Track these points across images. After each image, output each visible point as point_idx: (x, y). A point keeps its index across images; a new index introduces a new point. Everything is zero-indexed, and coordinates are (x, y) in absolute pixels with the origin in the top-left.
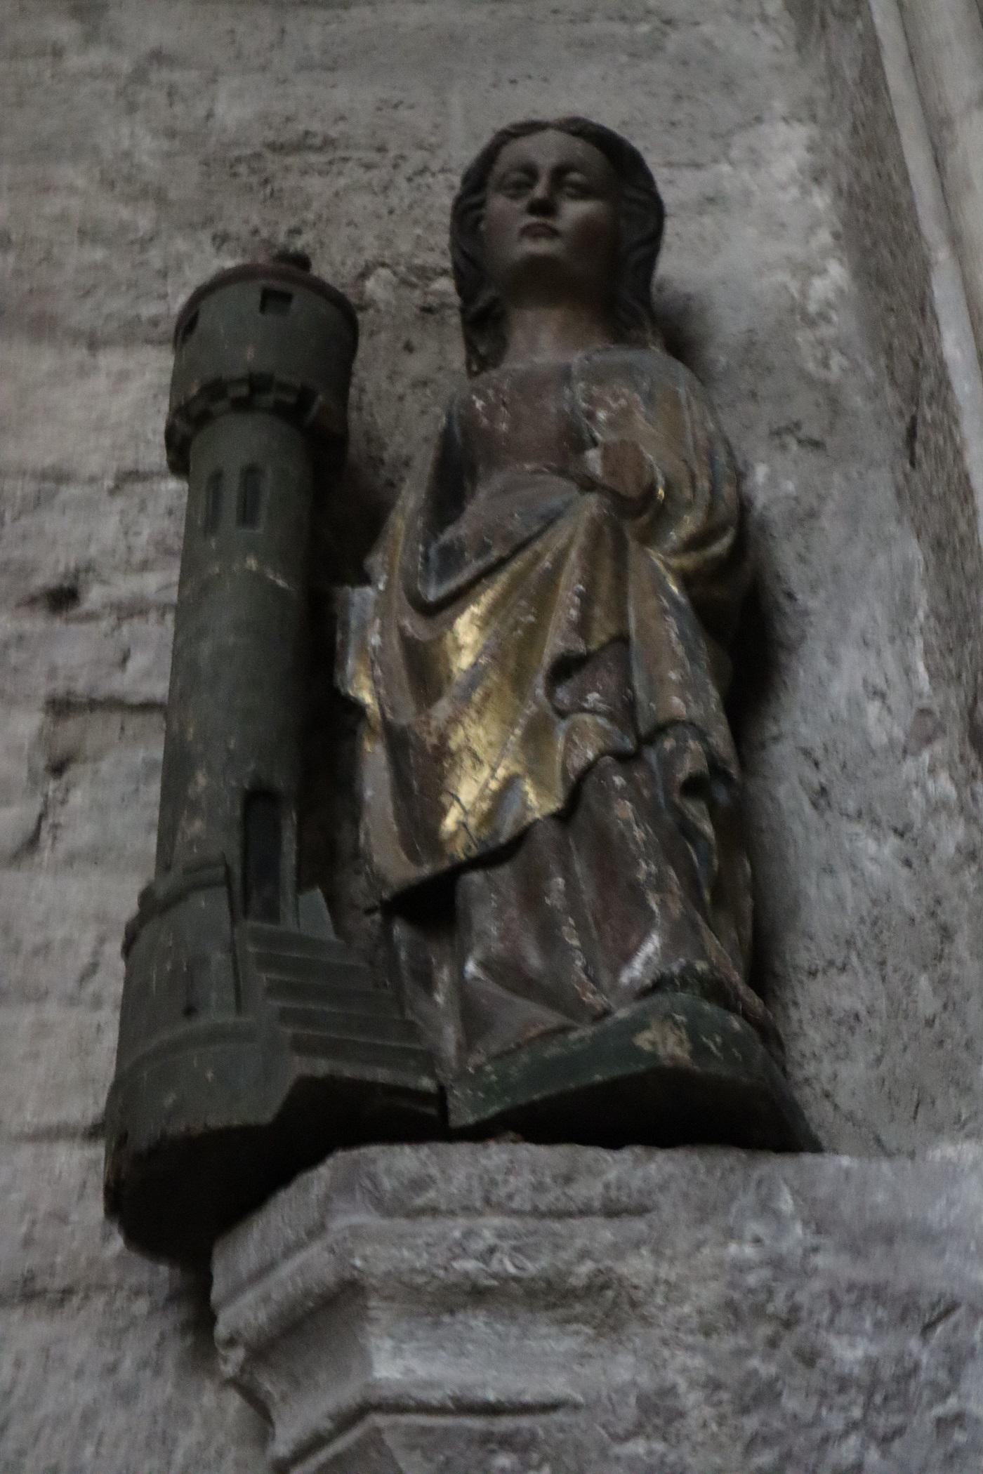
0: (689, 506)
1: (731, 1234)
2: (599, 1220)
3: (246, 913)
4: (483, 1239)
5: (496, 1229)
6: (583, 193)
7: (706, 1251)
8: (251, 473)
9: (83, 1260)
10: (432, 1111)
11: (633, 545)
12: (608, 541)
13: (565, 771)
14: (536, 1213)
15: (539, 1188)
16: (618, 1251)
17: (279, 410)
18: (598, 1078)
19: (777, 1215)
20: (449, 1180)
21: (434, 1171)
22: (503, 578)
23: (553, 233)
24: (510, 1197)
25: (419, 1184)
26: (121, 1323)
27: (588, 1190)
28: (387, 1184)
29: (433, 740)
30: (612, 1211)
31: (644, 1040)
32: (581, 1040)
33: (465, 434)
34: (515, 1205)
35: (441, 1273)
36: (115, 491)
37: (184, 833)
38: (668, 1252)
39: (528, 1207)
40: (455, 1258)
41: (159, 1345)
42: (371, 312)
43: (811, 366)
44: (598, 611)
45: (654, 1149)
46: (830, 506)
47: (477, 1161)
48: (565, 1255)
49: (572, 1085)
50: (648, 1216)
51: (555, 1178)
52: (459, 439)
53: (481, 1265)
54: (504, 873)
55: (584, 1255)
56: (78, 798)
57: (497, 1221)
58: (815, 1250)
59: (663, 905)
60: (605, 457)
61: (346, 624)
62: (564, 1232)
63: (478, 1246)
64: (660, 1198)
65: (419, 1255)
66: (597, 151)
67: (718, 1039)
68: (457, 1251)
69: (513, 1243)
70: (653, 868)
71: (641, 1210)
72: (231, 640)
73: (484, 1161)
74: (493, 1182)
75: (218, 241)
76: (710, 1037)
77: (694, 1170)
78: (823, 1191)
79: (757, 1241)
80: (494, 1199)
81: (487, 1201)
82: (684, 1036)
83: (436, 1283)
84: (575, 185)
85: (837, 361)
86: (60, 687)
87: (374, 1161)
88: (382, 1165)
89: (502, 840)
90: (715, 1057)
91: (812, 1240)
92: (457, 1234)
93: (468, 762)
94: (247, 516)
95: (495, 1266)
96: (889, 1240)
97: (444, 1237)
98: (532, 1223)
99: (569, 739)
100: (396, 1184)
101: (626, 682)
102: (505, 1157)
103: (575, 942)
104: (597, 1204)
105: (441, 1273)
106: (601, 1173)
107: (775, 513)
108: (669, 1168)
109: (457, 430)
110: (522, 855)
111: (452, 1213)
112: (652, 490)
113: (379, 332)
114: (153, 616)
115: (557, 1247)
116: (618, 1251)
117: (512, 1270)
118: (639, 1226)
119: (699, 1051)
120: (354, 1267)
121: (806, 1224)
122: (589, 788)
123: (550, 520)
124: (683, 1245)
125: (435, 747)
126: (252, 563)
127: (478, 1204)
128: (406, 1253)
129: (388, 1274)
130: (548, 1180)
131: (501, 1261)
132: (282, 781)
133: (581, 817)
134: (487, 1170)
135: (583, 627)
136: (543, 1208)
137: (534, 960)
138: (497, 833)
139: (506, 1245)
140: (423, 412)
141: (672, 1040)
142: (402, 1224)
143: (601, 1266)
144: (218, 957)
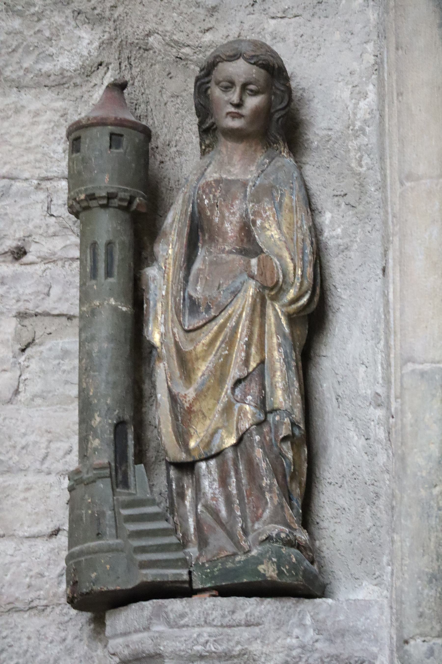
0: (292, 285)
1: (288, 634)
2: (243, 628)
3: (117, 487)
4: (204, 637)
5: (209, 633)
6: (255, 93)
7: (279, 641)
8: (109, 244)
9: (51, 594)
10: (187, 585)
11: (268, 302)
12: (258, 307)
13: (237, 429)
14: (222, 626)
15: (223, 616)
16: (249, 641)
17: (120, 207)
18: (245, 580)
20: (192, 614)
21: (187, 610)
22: (215, 327)
23: (240, 116)
24: (213, 620)
25: (182, 616)
26: (66, 618)
27: (240, 616)
28: (172, 616)
29: (187, 405)
30: (248, 625)
31: (261, 568)
32: (239, 562)
33: (199, 212)
34: (215, 623)
35: (190, 651)
36: (38, 187)
37: (92, 444)
38: (266, 642)
39: (219, 624)
40: (195, 645)
41: (81, 629)
42: (151, 52)
43: (354, 164)
44: (253, 350)
45: (263, 599)
46: (355, 246)
47: (202, 606)
48: (232, 644)
49: (236, 582)
50: (260, 627)
51: (229, 612)
52: (197, 215)
53: (203, 648)
54: (212, 462)
55: (238, 643)
56: (34, 365)
57: (209, 629)
58: (317, 641)
59: (271, 498)
60: (258, 265)
61: (148, 299)
62: (232, 634)
63: (202, 640)
65: (182, 645)
66: (262, 71)
67: (287, 567)
68: (195, 642)
69: (214, 638)
70: (268, 482)
71: (258, 624)
72: (105, 345)
73: (205, 606)
74: (208, 614)
75: (76, 14)
76: (284, 567)
77: (277, 608)
78: (321, 616)
79: (297, 637)
80: (208, 621)
81: (205, 622)
82: (275, 568)
83: (188, 654)
84: (251, 91)
85: (366, 160)
86: (22, 307)
87: (166, 607)
88: (170, 608)
89: (213, 453)
90: (285, 575)
91: (317, 637)
92: (195, 635)
93: (201, 416)
94: (109, 274)
95: (208, 648)
96: (343, 635)
97: (191, 637)
98: (220, 629)
99: (239, 415)
100: (174, 615)
101: (263, 387)
102: (212, 603)
103: (239, 513)
104: (243, 622)
105: (190, 651)
106: (245, 609)
107: (331, 243)
108: (268, 607)
109: (196, 209)
110: (220, 457)
111: (193, 626)
112: (278, 282)
113: (155, 65)
115: (229, 640)
116: (249, 641)
117: (213, 649)
118: (257, 630)
119: (280, 573)
120: (161, 650)
121: (314, 630)
122: (245, 437)
123: (235, 294)
124: (272, 639)
125: (188, 408)
126: (112, 301)
128: (178, 644)
129: (172, 652)
130: (226, 613)
131: (210, 646)
132: (127, 417)
133: (242, 445)
134: (205, 609)
135: (246, 362)
136: (224, 624)
137: (223, 512)
139: (212, 639)
140: (177, 113)
141: (271, 569)
143: (244, 648)
144: (109, 513)
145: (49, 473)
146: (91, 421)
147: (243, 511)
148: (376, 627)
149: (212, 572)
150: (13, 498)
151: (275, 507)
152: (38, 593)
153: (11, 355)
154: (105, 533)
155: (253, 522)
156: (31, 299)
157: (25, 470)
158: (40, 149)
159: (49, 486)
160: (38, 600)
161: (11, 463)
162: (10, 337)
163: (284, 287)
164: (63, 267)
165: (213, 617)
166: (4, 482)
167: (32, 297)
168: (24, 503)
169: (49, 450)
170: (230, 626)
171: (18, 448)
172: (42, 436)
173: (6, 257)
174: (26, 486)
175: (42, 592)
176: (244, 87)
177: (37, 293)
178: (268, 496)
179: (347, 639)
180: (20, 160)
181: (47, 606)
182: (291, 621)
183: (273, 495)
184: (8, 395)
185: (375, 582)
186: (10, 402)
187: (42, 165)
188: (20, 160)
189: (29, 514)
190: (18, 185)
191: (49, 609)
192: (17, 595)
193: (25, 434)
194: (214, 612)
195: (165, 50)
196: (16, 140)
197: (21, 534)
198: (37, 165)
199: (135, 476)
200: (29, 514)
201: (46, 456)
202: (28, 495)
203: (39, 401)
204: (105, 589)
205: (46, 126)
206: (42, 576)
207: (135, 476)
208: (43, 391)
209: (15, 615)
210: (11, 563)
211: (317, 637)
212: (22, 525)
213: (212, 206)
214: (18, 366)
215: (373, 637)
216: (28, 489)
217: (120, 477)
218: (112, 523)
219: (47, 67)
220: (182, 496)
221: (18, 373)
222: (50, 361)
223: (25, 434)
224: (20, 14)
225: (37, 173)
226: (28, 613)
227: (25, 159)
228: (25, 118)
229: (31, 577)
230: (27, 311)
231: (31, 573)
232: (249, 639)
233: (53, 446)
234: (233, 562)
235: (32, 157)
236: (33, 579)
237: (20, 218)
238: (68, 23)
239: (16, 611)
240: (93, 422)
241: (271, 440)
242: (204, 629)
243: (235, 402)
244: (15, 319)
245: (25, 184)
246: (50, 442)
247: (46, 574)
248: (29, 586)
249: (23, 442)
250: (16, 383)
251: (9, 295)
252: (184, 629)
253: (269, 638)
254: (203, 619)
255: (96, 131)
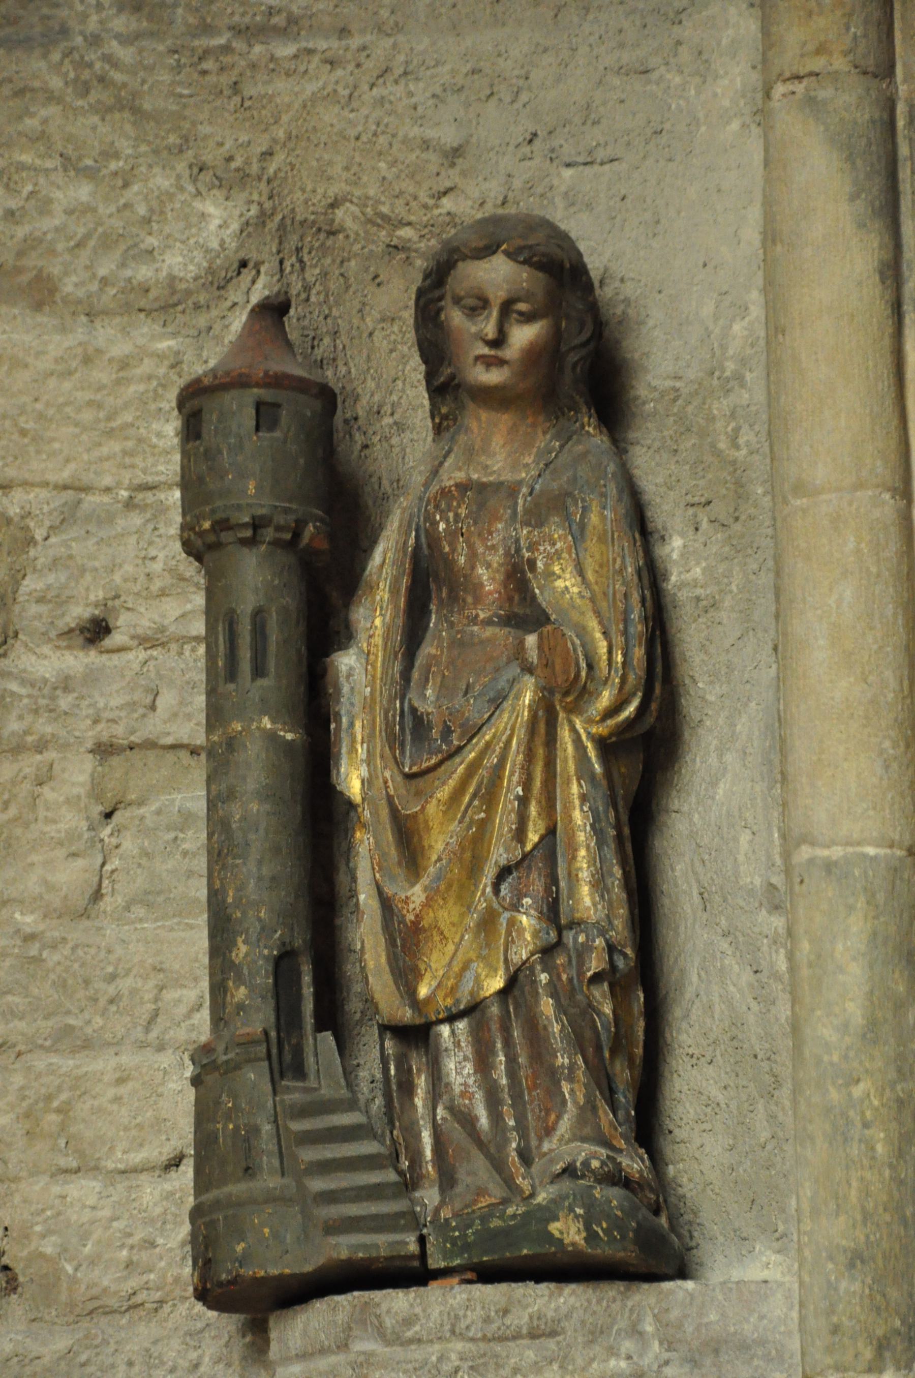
1: (612, 1352)
3: (282, 1076)
6: (528, 318)
8: (258, 615)
9: (170, 1279)
10: (416, 1263)
11: (562, 715)
13: (506, 960)
14: (484, 1338)
15: (487, 1320)
18: (525, 1251)
19: (641, 1334)
20: (428, 1317)
21: (418, 1310)
23: (501, 362)
24: (468, 1328)
25: (408, 1322)
26: (199, 1325)
27: (520, 1319)
28: (388, 1322)
29: (410, 917)
30: (534, 1335)
31: (555, 1228)
32: (514, 1216)
34: (471, 1334)
36: (129, 504)
37: (233, 996)
38: (570, 1367)
39: (479, 1335)
41: (227, 1345)
42: (341, 236)
44: (533, 810)
45: (563, 1285)
47: (447, 1302)
51: (497, 1312)
52: (426, 551)
54: (462, 1025)
56: (129, 844)
57: (459, 1346)
58: (667, 1363)
59: (572, 1091)
60: (540, 647)
61: (338, 715)
62: (504, 1354)
64: (565, 1324)
66: (540, 275)
67: (604, 1225)
69: (470, 1364)
70: (566, 1061)
71: (553, 1334)
72: (254, 807)
73: (451, 1301)
74: (457, 1317)
75: (195, 170)
76: (600, 1225)
77: (589, 1301)
78: (675, 1314)
79: (629, 1358)
80: (457, 1331)
81: (453, 1332)
82: (581, 1227)
84: (521, 313)
86: (103, 732)
87: (378, 1305)
88: (384, 1307)
90: (601, 1239)
91: (666, 1355)
92: (434, 1358)
93: (437, 938)
94: (259, 671)
96: (716, 1351)
97: (426, 1362)
99: (509, 933)
101: (553, 879)
102: (464, 1296)
103: (512, 1123)
104: (524, 1331)
106: (527, 1306)
107: (683, 595)
108: (572, 1300)
109: (423, 539)
110: (477, 1014)
111: (431, 1341)
113: (349, 260)
114: (174, 647)
115: (498, 1366)
119: (591, 1237)
121: (661, 1343)
122: (521, 976)
123: (497, 702)
124: (580, 1362)
125: (412, 922)
126: (267, 723)
127: (448, 1335)
130: (493, 1314)
132: (298, 943)
133: (516, 992)
136: (489, 1335)
137: (484, 1121)
138: (458, 1001)
139: (466, 1365)
140: (391, 351)
141: (573, 1230)
142: (398, 1352)
144: (267, 1128)
145: (161, 1048)
146: (230, 952)
147: (521, 1120)
148: (780, 1333)
149: (464, 1236)
150: (95, 1098)
151: (581, 1109)
152: (145, 1278)
153: (84, 825)
154: (260, 1168)
155: (540, 1140)
156: (120, 718)
157: (117, 1044)
158: (132, 432)
159: (161, 1073)
160: (145, 1292)
161: (89, 1030)
162: (81, 791)
163: (591, 687)
164: (180, 654)
165: (468, 1321)
166: (78, 1067)
167: (123, 714)
168: (115, 1107)
169: (160, 1004)
170: (502, 1339)
171: (102, 1002)
172: (145, 978)
173: (71, 639)
174: (117, 1075)
175: (152, 1276)
176: (506, 308)
177: (132, 706)
178: (566, 1087)
179: (724, 1358)
180: (96, 454)
181: (161, 1302)
182: (616, 1328)
183: (576, 1086)
184: (81, 902)
185: (776, 1245)
186: (85, 914)
187: (138, 460)
188: (96, 454)
189: (126, 1129)
190: (92, 500)
191: (167, 1308)
192: (105, 1283)
193: (113, 977)
194: (469, 1313)
195: (366, 232)
196: (87, 416)
197: (110, 1165)
198: (127, 460)
199: (316, 1055)
200: (126, 1129)
201: (155, 1015)
202: (123, 1090)
203: (139, 911)
204: (262, 1273)
205: (142, 388)
206: (153, 1245)
207: (316, 1055)
208: (147, 893)
209: (104, 1320)
210: (92, 1222)
211: (666, 1355)
212: (112, 1149)
213: (453, 534)
214: (99, 846)
215: (774, 1352)
216: (120, 1081)
217: (288, 1057)
218: (272, 1147)
219: (144, 273)
220: (407, 1088)
221: (100, 861)
222: (160, 834)
223: (113, 977)
224: (90, 174)
225: (126, 477)
226: (127, 1315)
227: (105, 450)
228: (102, 375)
229: (132, 1247)
230: (114, 740)
231: (130, 1241)
232: (536, 1363)
233: (170, 995)
234: (501, 1217)
235: (115, 446)
236: (135, 1251)
237: (97, 564)
238: (182, 189)
239: (106, 1313)
240: (234, 954)
241: (570, 980)
242: (450, 1346)
243: (501, 910)
244: (91, 756)
245: (106, 499)
246: (161, 989)
247: (160, 1241)
248: (129, 1265)
249: (111, 990)
250: (96, 879)
251: (77, 711)
252: (413, 1347)
253: (573, 1360)
254: (447, 1327)
255: (230, 400)
